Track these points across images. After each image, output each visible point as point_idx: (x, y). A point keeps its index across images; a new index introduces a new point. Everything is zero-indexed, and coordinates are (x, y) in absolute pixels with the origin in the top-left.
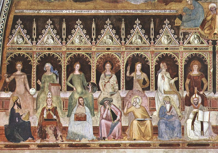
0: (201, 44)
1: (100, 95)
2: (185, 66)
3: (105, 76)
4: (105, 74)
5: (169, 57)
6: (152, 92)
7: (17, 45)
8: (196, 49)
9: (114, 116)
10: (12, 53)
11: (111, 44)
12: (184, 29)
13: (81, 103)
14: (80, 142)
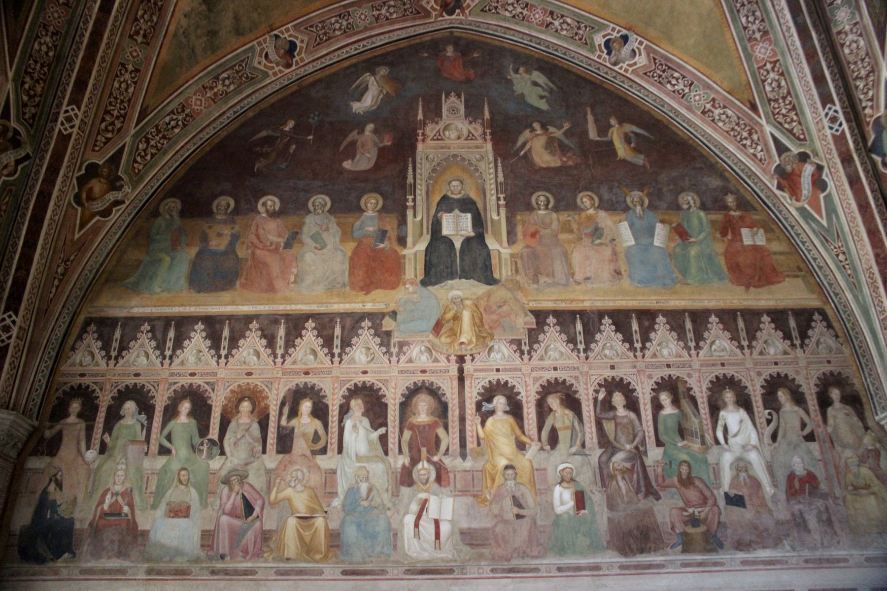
0: (434, 362)
6: (330, 458)
7: (80, 368)
8: (423, 372)
9: (249, 508)
10: (65, 383)
14: (171, 565)
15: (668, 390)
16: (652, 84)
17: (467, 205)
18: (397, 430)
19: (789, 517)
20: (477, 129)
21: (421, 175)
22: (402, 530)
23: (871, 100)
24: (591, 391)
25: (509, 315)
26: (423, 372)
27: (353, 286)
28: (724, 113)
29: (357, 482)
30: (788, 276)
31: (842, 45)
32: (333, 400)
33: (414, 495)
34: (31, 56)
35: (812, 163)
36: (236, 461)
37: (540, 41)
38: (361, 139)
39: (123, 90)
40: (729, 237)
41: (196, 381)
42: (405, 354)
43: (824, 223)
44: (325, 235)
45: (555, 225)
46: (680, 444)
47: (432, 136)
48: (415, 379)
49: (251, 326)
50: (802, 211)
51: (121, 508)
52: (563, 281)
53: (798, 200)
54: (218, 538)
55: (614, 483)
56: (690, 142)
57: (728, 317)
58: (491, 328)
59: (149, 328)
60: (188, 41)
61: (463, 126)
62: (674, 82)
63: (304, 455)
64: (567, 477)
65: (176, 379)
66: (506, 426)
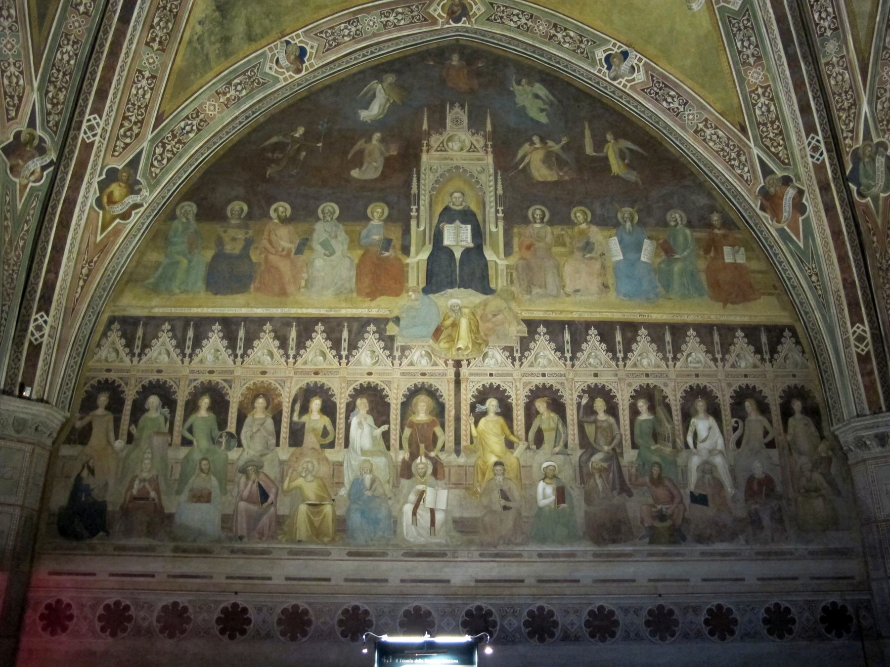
2: (403, 404)
7: (106, 364)
8: (423, 374)
9: (264, 495)
10: (93, 378)
14: (195, 545)
15: (645, 398)
16: (649, 101)
17: (467, 216)
18: (398, 427)
19: (745, 515)
20: (479, 141)
21: (425, 185)
22: (401, 518)
23: (852, 131)
24: (575, 396)
25: (503, 323)
26: (423, 374)
27: (359, 292)
28: (715, 134)
29: (361, 474)
30: (764, 294)
31: (829, 76)
32: (341, 398)
33: (411, 487)
34: (54, 65)
35: (794, 187)
36: (252, 452)
37: (542, 52)
38: (369, 147)
39: (140, 96)
40: (712, 254)
41: (214, 378)
43: (801, 245)
44: (333, 242)
45: (549, 238)
46: (653, 448)
47: (436, 146)
48: (416, 381)
49: (264, 328)
50: (781, 232)
51: (148, 493)
52: (554, 293)
53: (778, 222)
54: (237, 522)
55: (592, 481)
56: (682, 159)
57: (705, 331)
58: (486, 335)
59: (169, 327)
60: (202, 48)
61: (465, 137)
62: (670, 100)
64: (550, 473)
65: (195, 376)
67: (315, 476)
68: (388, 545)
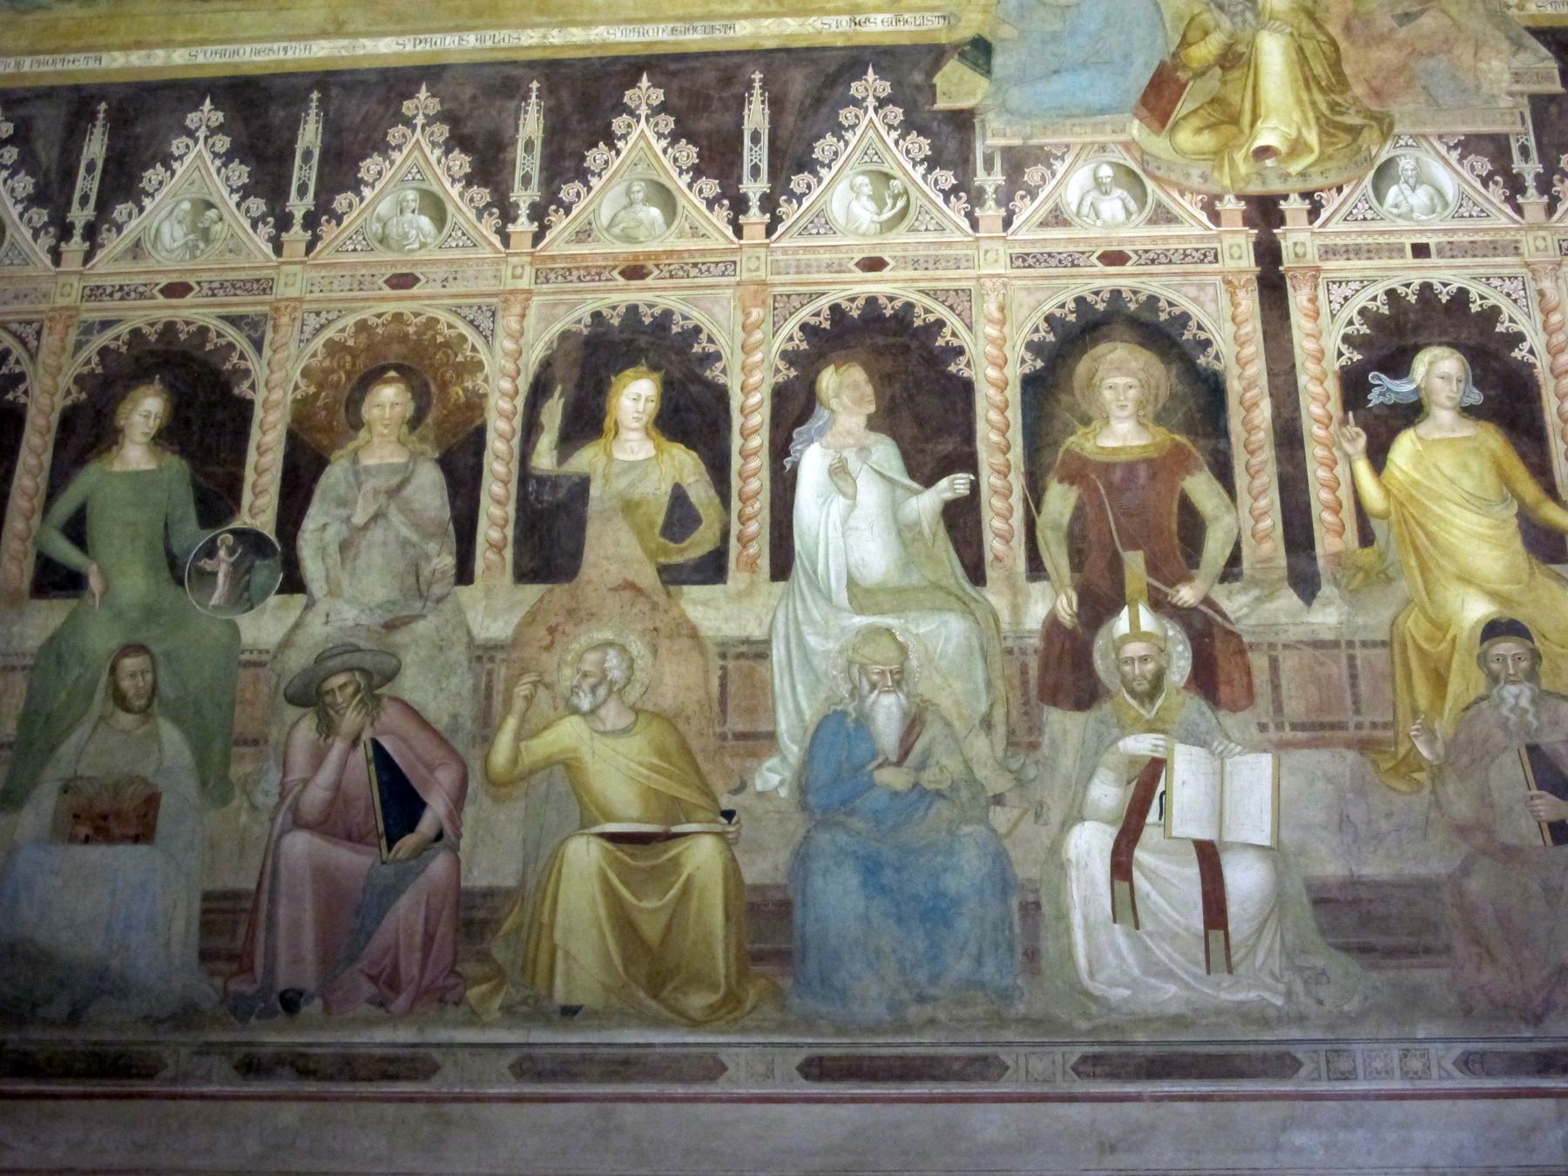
0: (1152, 221)
1: (297, 626)
3: (356, 474)
4: (355, 461)
5: (893, 323)
6: (740, 596)
8: (1115, 258)
11: (423, 245)
12: (1008, 131)
13: (131, 693)
18: (1017, 482)
25: (1448, 44)
29: (854, 692)
36: (349, 614)
41: (187, 314)
42: (1032, 193)
48: (1083, 287)
49: (408, 107)
58: (1377, 94)
63: (630, 586)
65: (110, 308)
66: (1474, 465)
67: (636, 711)
68: (1002, 1022)
